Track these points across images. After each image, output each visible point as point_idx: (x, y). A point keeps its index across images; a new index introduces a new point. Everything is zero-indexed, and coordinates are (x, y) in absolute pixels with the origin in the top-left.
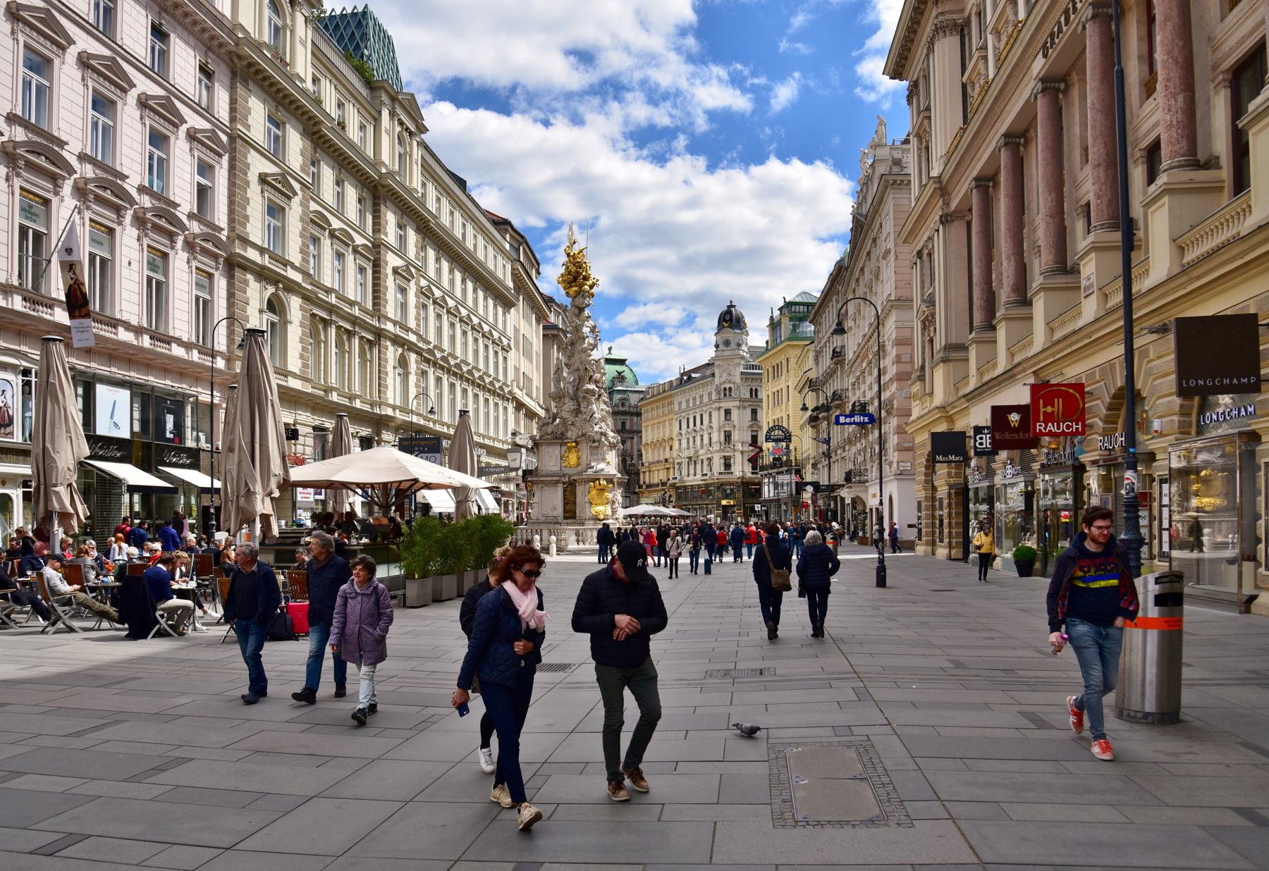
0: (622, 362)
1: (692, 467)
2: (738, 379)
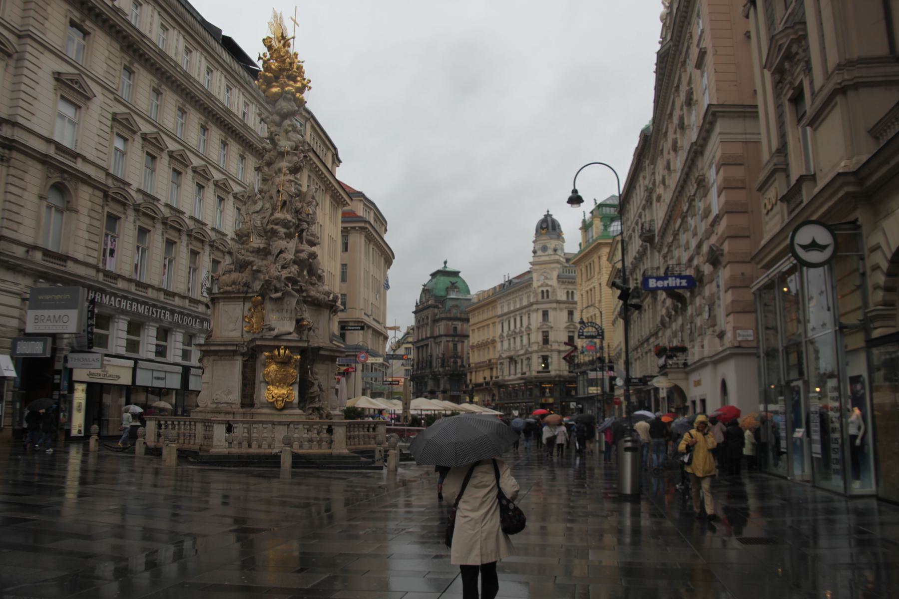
0: (456, 274)
1: (513, 367)
2: (554, 282)
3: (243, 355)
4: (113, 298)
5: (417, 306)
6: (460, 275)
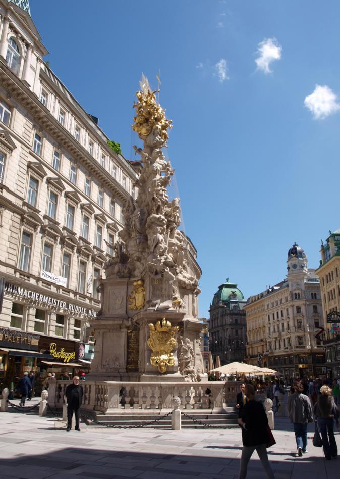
0: (234, 286)
3: (128, 328)
4: (26, 290)
5: (211, 307)
6: (237, 287)
